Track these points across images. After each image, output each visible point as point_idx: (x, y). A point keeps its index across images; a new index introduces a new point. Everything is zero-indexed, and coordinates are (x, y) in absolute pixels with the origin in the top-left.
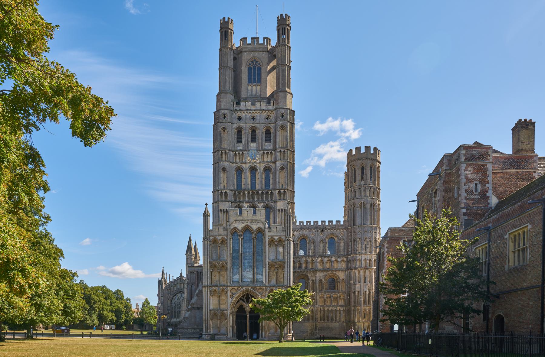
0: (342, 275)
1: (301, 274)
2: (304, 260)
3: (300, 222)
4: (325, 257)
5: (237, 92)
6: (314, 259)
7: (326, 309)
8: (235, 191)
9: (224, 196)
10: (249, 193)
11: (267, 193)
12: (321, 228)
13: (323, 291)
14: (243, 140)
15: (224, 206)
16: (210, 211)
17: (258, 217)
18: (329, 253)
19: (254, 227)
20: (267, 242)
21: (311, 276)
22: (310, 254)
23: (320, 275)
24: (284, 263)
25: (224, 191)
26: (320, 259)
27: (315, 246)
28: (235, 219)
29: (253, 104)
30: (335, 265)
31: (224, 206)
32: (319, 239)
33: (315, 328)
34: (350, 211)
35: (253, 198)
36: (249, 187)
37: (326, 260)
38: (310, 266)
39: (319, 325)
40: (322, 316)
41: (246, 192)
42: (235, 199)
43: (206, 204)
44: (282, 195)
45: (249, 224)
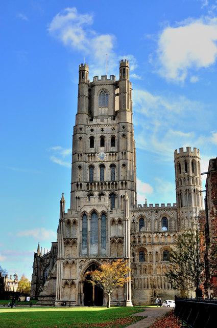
1: (140, 247)
2: (142, 235)
3: (139, 205)
4: (160, 233)
6: (150, 234)
7: (162, 277)
8: (88, 183)
9: (79, 186)
10: (98, 184)
11: (113, 184)
13: (159, 262)
17: (102, 202)
19: (99, 210)
20: (109, 222)
21: (148, 249)
22: (148, 230)
23: (157, 248)
24: (123, 238)
25: (79, 183)
26: (155, 235)
27: (151, 224)
28: (84, 204)
31: (79, 194)
32: (154, 218)
33: (154, 294)
34: (179, 195)
35: (102, 188)
36: (99, 180)
37: (160, 235)
38: (148, 240)
39: (157, 293)
40: (159, 284)
41: (97, 183)
42: (88, 189)
43: (63, 194)
44: (124, 185)
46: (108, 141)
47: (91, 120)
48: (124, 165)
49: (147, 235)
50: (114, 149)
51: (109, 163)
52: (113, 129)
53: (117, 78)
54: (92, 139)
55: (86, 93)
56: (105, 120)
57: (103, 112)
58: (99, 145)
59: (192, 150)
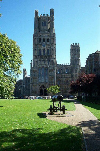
0: (70, 79)
5: (39, 29)
10: (43, 56)
12: (64, 66)
14: (41, 42)
15: (36, 60)
16: (32, 62)
18: (66, 72)
19: (45, 66)
23: (64, 79)
29: (44, 32)
30: (68, 76)
34: (72, 61)
36: (43, 54)
37: (65, 75)
44: (52, 57)
45: (44, 66)
46: (46, 40)
47: (40, 32)
48: (52, 49)
49: (61, 75)
50: (49, 43)
51: (47, 49)
52: (48, 35)
53: (49, 16)
54: (40, 39)
55: (38, 21)
56: (45, 32)
57: (44, 29)
58: (43, 41)
59: (77, 44)
